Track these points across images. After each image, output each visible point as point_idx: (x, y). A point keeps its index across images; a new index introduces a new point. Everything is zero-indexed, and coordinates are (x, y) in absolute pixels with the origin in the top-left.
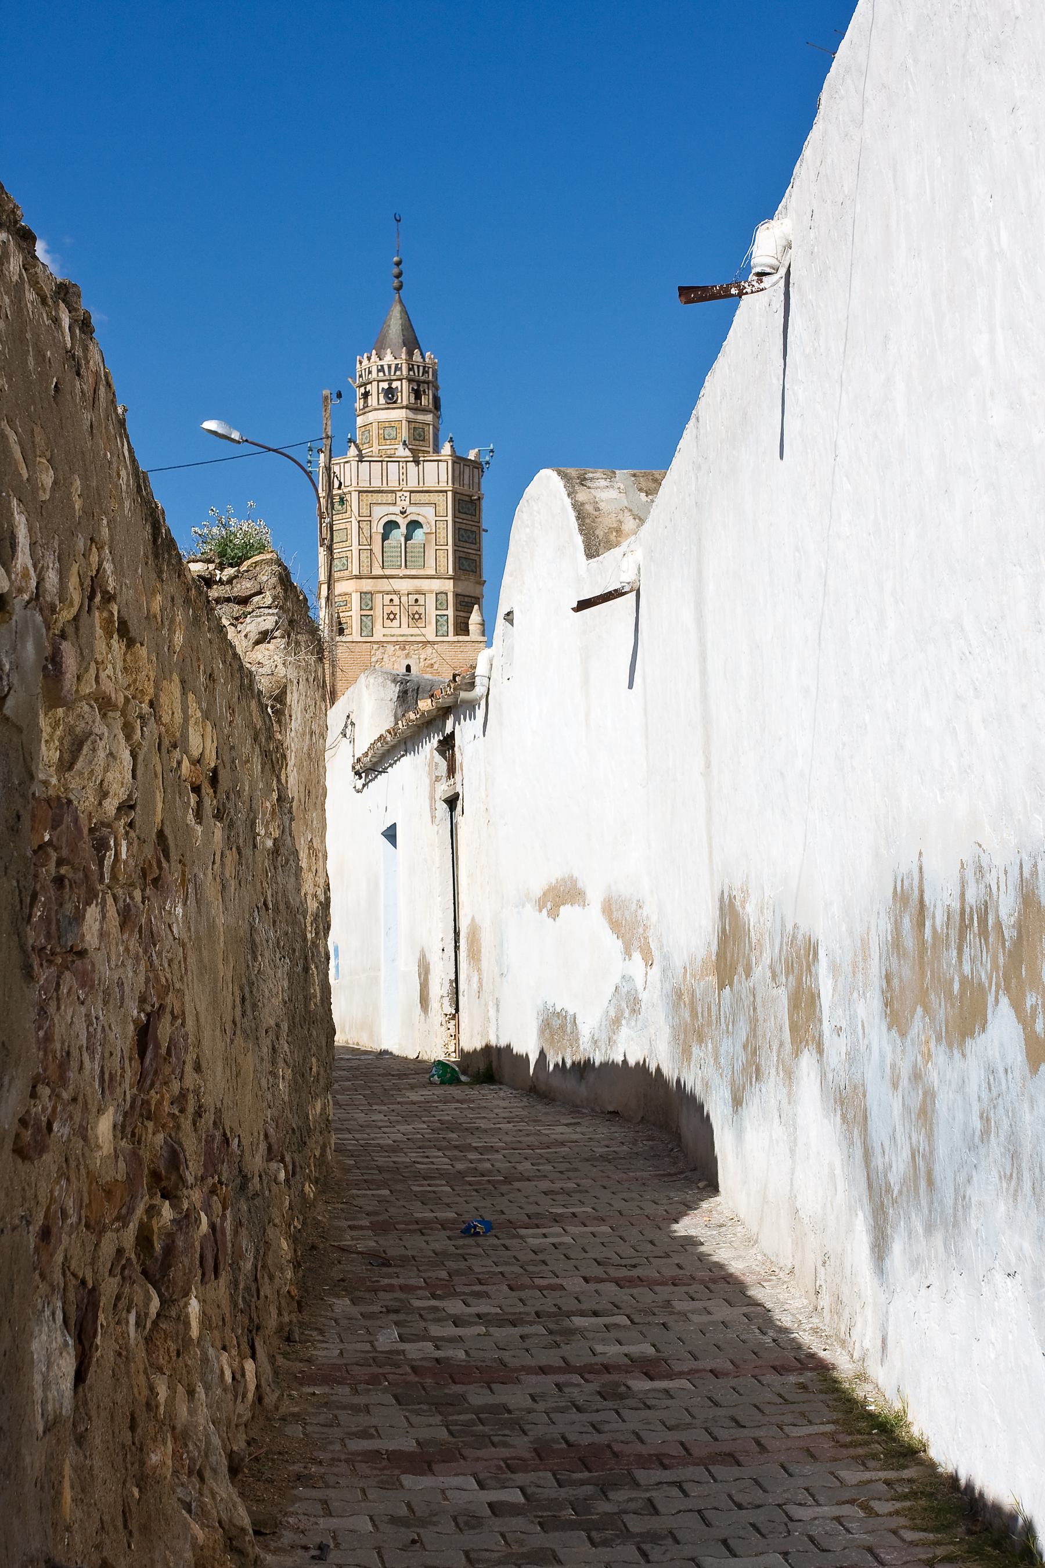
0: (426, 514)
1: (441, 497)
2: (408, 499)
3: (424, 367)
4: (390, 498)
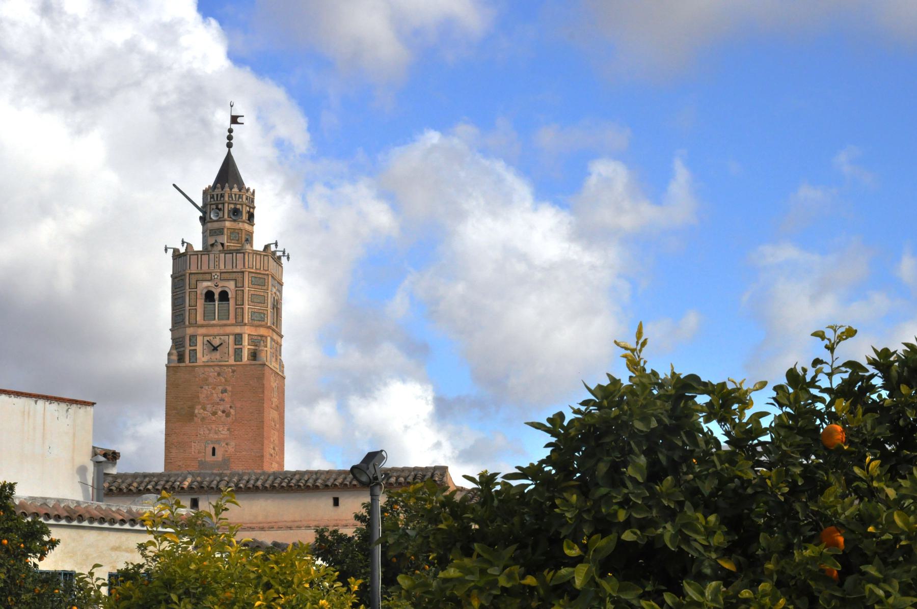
0: (230, 286)
1: (240, 275)
4: (208, 277)
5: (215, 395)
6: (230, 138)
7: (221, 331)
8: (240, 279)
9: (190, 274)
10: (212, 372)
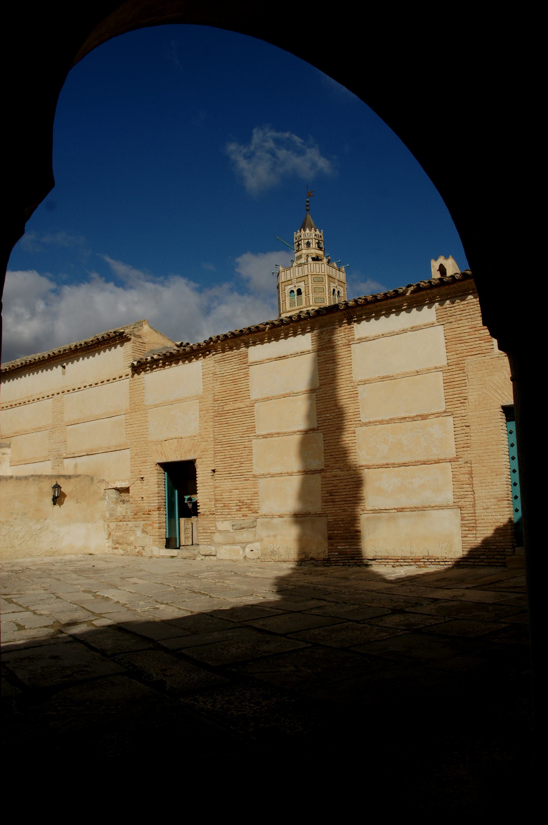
0: (302, 286)
4: (290, 282)
8: (306, 280)
9: (282, 283)
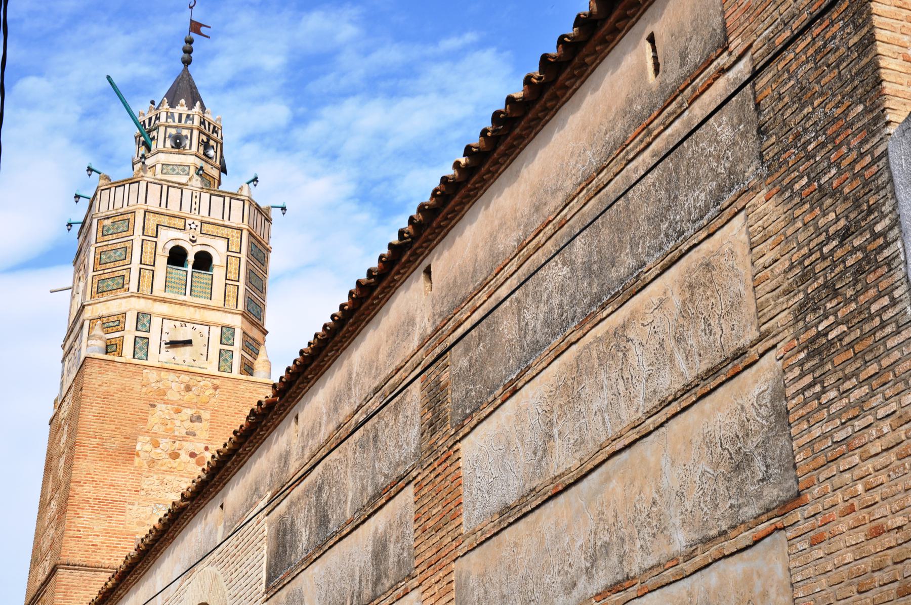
2: (198, 229)
3: (215, 127)
4: (179, 223)
5: (178, 423)
6: (188, 51)
7: (199, 315)
8: (235, 241)
10: (174, 385)
